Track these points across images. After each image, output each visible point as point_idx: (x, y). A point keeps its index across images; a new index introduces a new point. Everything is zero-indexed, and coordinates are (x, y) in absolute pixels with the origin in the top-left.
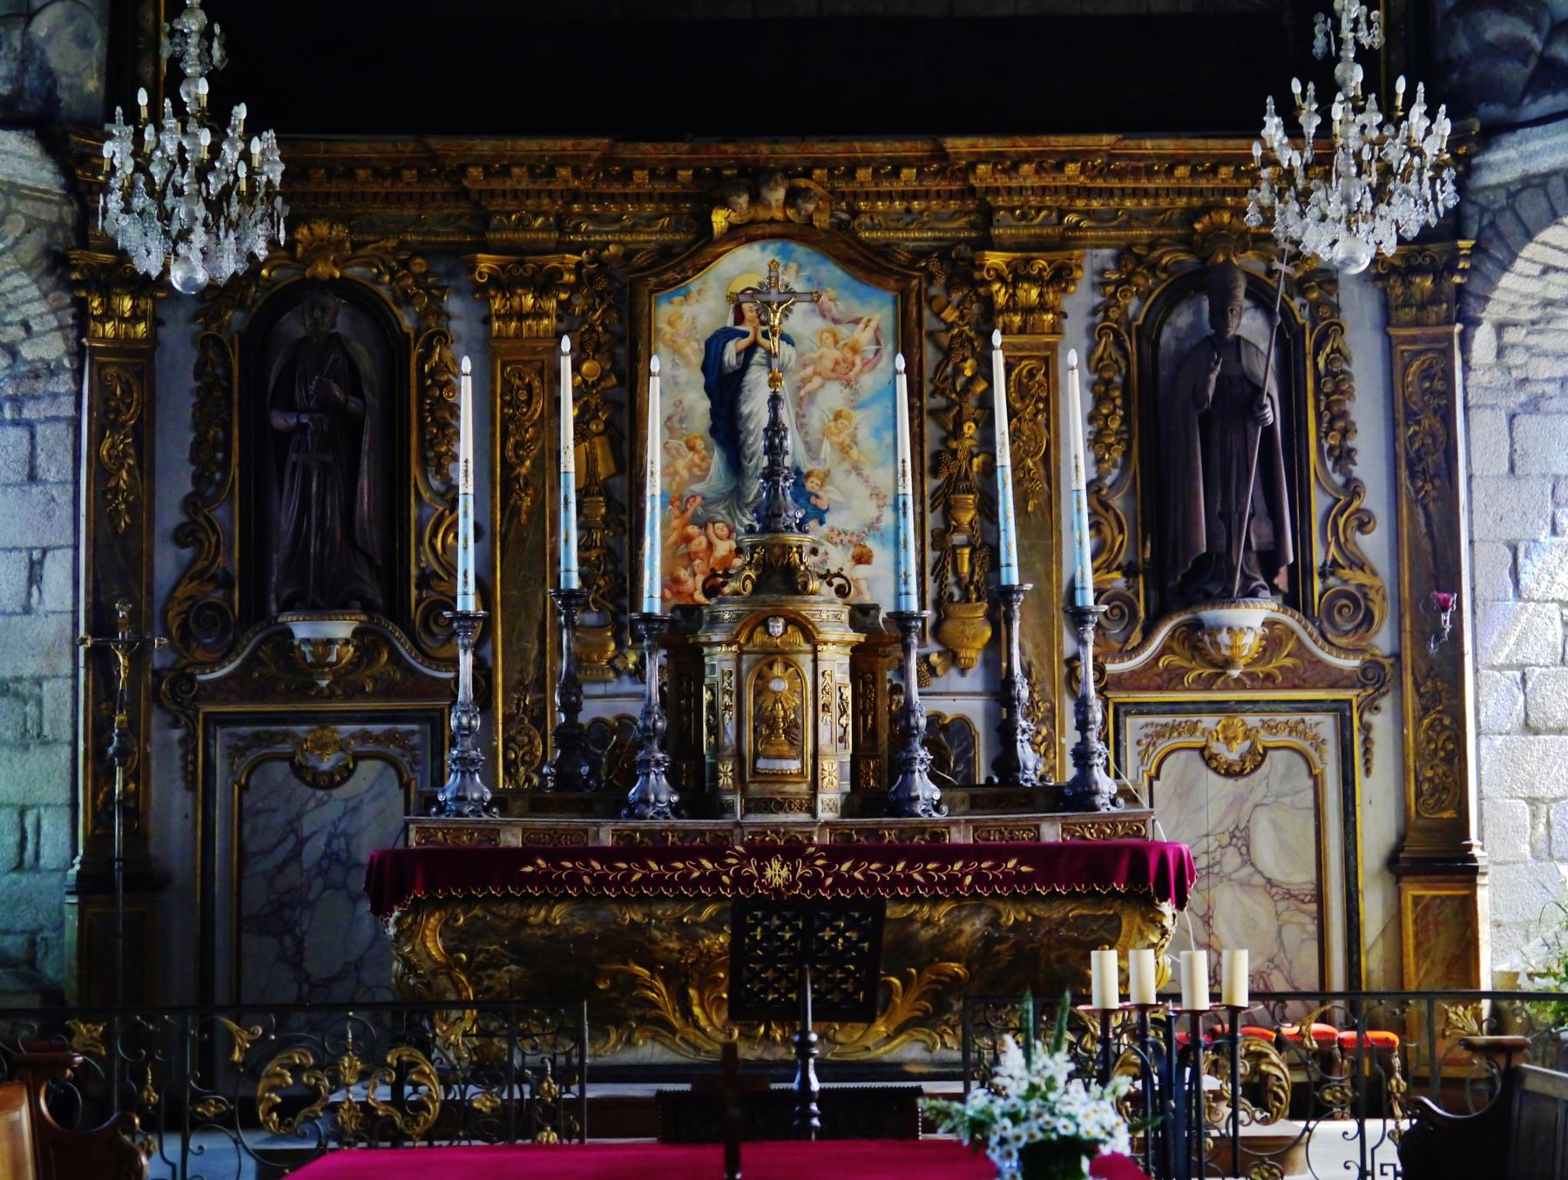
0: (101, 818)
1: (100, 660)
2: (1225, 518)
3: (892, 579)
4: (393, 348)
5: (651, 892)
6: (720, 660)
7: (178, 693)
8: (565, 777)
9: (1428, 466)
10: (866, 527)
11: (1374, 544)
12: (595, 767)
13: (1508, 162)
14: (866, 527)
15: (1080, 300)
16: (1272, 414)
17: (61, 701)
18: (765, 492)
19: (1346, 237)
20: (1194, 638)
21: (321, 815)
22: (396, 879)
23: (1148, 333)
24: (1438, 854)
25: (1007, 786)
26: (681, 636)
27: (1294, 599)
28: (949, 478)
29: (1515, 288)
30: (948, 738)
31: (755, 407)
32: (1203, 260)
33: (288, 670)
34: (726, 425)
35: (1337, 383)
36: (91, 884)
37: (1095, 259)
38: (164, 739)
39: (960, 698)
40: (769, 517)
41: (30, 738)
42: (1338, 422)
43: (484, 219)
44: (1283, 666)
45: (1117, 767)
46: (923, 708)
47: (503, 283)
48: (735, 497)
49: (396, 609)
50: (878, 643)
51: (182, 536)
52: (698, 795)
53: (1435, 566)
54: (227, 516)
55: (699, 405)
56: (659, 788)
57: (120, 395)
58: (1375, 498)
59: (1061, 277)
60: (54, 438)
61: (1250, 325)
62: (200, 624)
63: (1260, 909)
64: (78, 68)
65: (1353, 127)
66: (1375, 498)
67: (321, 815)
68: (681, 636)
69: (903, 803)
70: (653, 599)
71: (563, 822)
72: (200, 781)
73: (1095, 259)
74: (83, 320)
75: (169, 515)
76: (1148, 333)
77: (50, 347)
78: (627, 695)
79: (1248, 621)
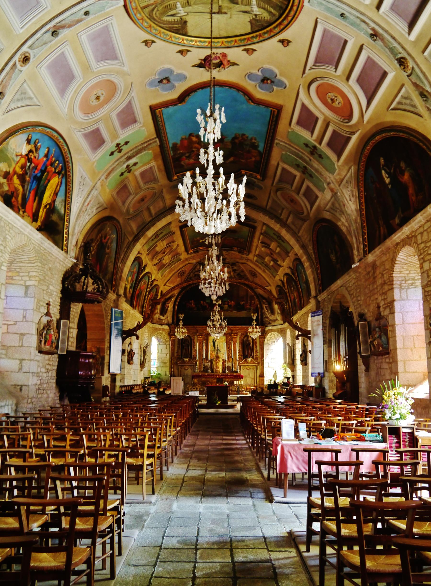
0: (171, 372)
1: (171, 361)
2: (248, 353)
3: (225, 357)
4: (191, 340)
5: (210, 378)
6: (214, 363)
7: (176, 363)
8: (204, 370)
9: (262, 349)
10: (223, 354)
11: (258, 354)
12: (206, 369)
13: (267, 328)
14: (223, 354)
15: (238, 337)
16: (251, 345)
17: (169, 364)
20: (246, 361)
21: (186, 372)
22: (193, 377)
24: (262, 376)
25: (232, 371)
26: (211, 361)
27: (253, 358)
28: (229, 349)
29: (268, 337)
30: (229, 367)
31: (216, 344)
32: (246, 335)
33: (184, 362)
34: (214, 345)
35: (256, 343)
37: (239, 334)
38: (175, 367)
39: (230, 364)
40: (217, 353)
41: (166, 366)
42: (256, 346)
43: (197, 331)
44: (252, 362)
45: (240, 369)
46: (227, 365)
47: (199, 335)
48: (215, 350)
49: (191, 358)
50: (224, 361)
51: (177, 352)
52: (212, 371)
53: (262, 356)
54: (180, 351)
55: (212, 344)
56: (210, 371)
57: (173, 343)
58: (258, 351)
59: (237, 335)
60: (168, 346)
61: (250, 339)
62: (178, 359)
63: (250, 379)
64: (171, 321)
65: (255, 330)
66: (258, 351)
67: (186, 372)
68: (211, 361)
69: (225, 372)
70: (209, 358)
71: (204, 373)
72: (178, 370)
73: (239, 334)
74: (170, 338)
75: (176, 351)
76: (243, 339)
77: (168, 340)
78: (208, 364)
79: (250, 360)
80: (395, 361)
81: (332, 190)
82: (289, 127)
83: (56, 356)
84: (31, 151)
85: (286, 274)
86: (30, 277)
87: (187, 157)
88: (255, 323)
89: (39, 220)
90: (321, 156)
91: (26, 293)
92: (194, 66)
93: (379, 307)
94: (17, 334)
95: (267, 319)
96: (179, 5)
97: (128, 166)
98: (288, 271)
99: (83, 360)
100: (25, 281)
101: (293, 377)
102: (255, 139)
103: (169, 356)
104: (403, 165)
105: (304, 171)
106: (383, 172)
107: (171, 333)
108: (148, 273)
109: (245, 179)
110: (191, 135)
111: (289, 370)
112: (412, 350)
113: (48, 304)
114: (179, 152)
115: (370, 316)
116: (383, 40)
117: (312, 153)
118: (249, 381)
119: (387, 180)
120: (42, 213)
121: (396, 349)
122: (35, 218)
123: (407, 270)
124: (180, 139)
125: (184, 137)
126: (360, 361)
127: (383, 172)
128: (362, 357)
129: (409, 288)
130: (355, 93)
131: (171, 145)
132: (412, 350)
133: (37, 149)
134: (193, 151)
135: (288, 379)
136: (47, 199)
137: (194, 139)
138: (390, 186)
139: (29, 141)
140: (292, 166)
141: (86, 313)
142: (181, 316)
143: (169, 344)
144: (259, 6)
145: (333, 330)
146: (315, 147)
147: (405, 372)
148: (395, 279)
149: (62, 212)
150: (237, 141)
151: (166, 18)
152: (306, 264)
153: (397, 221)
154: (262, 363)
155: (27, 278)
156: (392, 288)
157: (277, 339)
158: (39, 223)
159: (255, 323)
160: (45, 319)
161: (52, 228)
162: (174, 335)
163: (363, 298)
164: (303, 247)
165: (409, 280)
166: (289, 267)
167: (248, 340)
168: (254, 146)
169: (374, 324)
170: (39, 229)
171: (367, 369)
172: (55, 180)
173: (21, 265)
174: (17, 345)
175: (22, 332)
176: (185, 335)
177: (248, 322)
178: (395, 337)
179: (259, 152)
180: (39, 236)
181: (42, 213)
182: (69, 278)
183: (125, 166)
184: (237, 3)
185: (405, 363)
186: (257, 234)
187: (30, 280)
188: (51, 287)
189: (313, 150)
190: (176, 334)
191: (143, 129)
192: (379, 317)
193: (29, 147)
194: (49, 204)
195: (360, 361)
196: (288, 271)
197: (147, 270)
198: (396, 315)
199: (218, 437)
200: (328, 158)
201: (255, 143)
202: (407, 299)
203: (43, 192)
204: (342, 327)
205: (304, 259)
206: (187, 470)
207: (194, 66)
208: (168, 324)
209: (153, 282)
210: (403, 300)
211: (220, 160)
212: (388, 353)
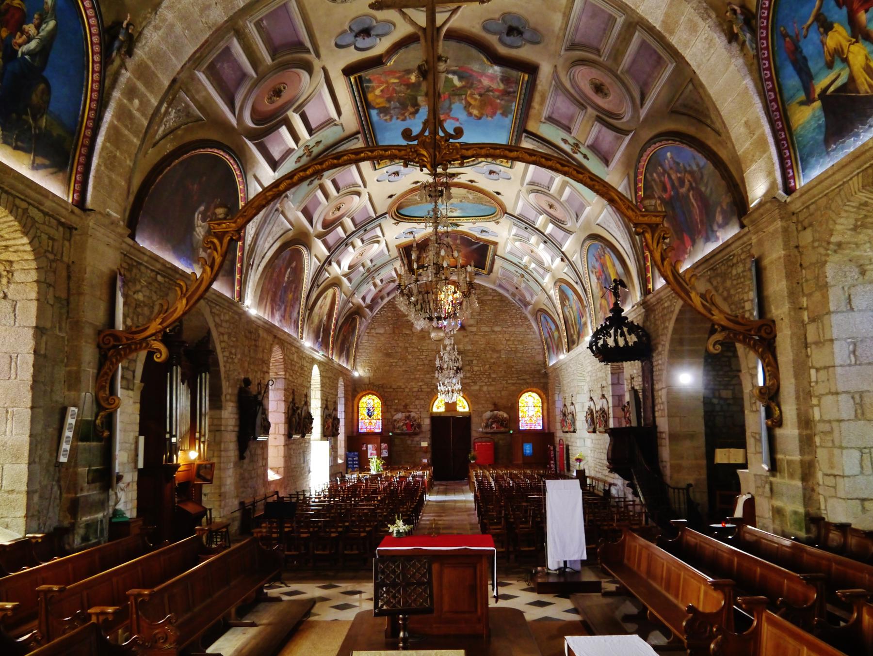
87: (491, 91)
102: (386, 120)
110: (480, 118)
114: (503, 102)
119: (286, 279)
124: (495, 118)
125: (489, 119)
131: (510, 116)
134: (481, 95)
137: (475, 112)
141: (707, 336)
150: (411, 109)
163: (239, 356)
168: (383, 111)
179: (374, 108)
199: (447, 522)
201: (385, 116)
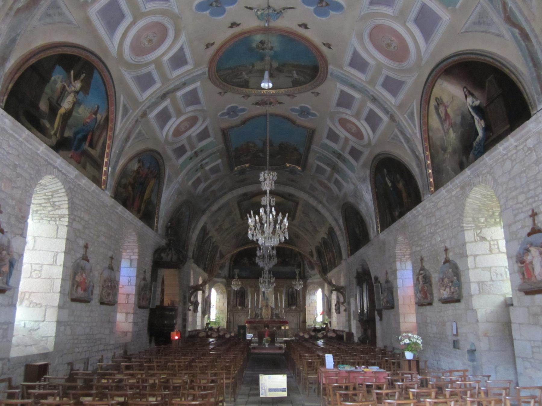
3: (273, 305)
4: (245, 291)
10: (272, 303)
15: (285, 288)
18: (266, 299)
19: (299, 288)
23: (288, 291)
24: (304, 322)
28: (276, 299)
29: (309, 288)
30: (276, 314)
34: (264, 295)
35: (299, 293)
36: (227, 322)
39: (277, 312)
40: (267, 302)
45: (286, 315)
51: (233, 301)
54: (235, 301)
58: (301, 300)
61: (294, 290)
77: (225, 290)
78: (259, 312)
79: (294, 308)
80: (398, 315)
81: (354, 184)
82: (322, 138)
83: (148, 310)
84: (139, 167)
85: (323, 238)
86: (133, 253)
88: (298, 277)
89: (141, 212)
90: (344, 161)
91: (131, 264)
92: (253, 104)
93: (387, 273)
94: (124, 294)
95: (308, 273)
96: (244, 73)
97: (201, 165)
98: (326, 237)
99: (168, 313)
100: (130, 256)
101: (330, 323)
103: (226, 304)
104: (398, 176)
105: (335, 168)
106: (387, 178)
107: (228, 286)
108: (211, 237)
109: (287, 214)
111: (327, 317)
112: (409, 306)
113: (145, 272)
115: (382, 279)
116: (379, 103)
117: (338, 158)
118: (293, 326)
119: (390, 185)
120: (143, 207)
121: (398, 305)
122: (139, 211)
123: (405, 248)
126: (376, 313)
127: (387, 178)
128: (377, 310)
129: (406, 261)
130: (364, 127)
132: (409, 306)
133: (143, 165)
135: (326, 324)
136: (146, 196)
138: (391, 189)
139: (139, 161)
140: (324, 163)
142: (236, 271)
143: (226, 295)
144: (298, 74)
145: (358, 287)
146: (340, 154)
147: (405, 322)
148: (397, 254)
149: (155, 203)
151: (235, 80)
152: (338, 233)
153: (397, 213)
154: (304, 311)
155: (131, 254)
156: (395, 261)
157: (316, 290)
158: (141, 214)
159: (298, 277)
160: (143, 283)
161: (147, 216)
162: (231, 287)
164: (336, 220)
165: (407, 255)
166: (326, 233)
167: (292, 291)
169: (384, 285)
170: (141, 219)
171: (381, 319)
172: (152, 182)
173: (128, 244)
174: (124, 302)
175: (128, 293)
176: (240, 286)
177: (292, 277)
178: (397, 296)
180: (140, 223)
181: (143, 207)
182: (158, 251)
183: (199, 165)
184: (283, 72)
185: (404, 316)
186: (300, 207)
187: (134, 255)
188: (146, 259)
189: (339, 156)
190: (232, 286)
191: (214, 140)
192: (387, 282)
193: (139, 165)
194: (148, 199)
195: (376, 313)
196: (326, 237)
197: (210, 235)
198: (398, 280)
200: (349, 162)
202: (406, 269)
203: (144, 192)
204: (365, 286)
205: (336, 229)
206: (251, 390)
207: (253, 104)
208: (225, 278)
209: (213, 243)
210: (402, 269)
211: (273, 203)
212: (392, 307)
